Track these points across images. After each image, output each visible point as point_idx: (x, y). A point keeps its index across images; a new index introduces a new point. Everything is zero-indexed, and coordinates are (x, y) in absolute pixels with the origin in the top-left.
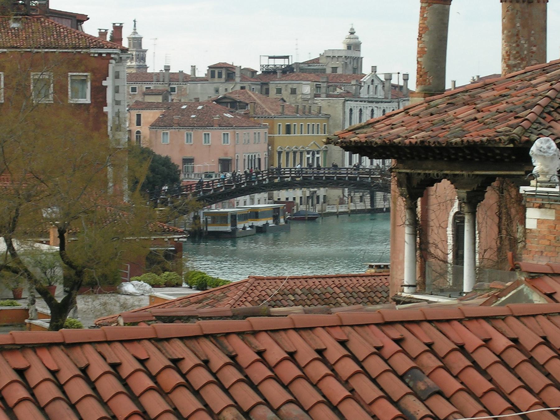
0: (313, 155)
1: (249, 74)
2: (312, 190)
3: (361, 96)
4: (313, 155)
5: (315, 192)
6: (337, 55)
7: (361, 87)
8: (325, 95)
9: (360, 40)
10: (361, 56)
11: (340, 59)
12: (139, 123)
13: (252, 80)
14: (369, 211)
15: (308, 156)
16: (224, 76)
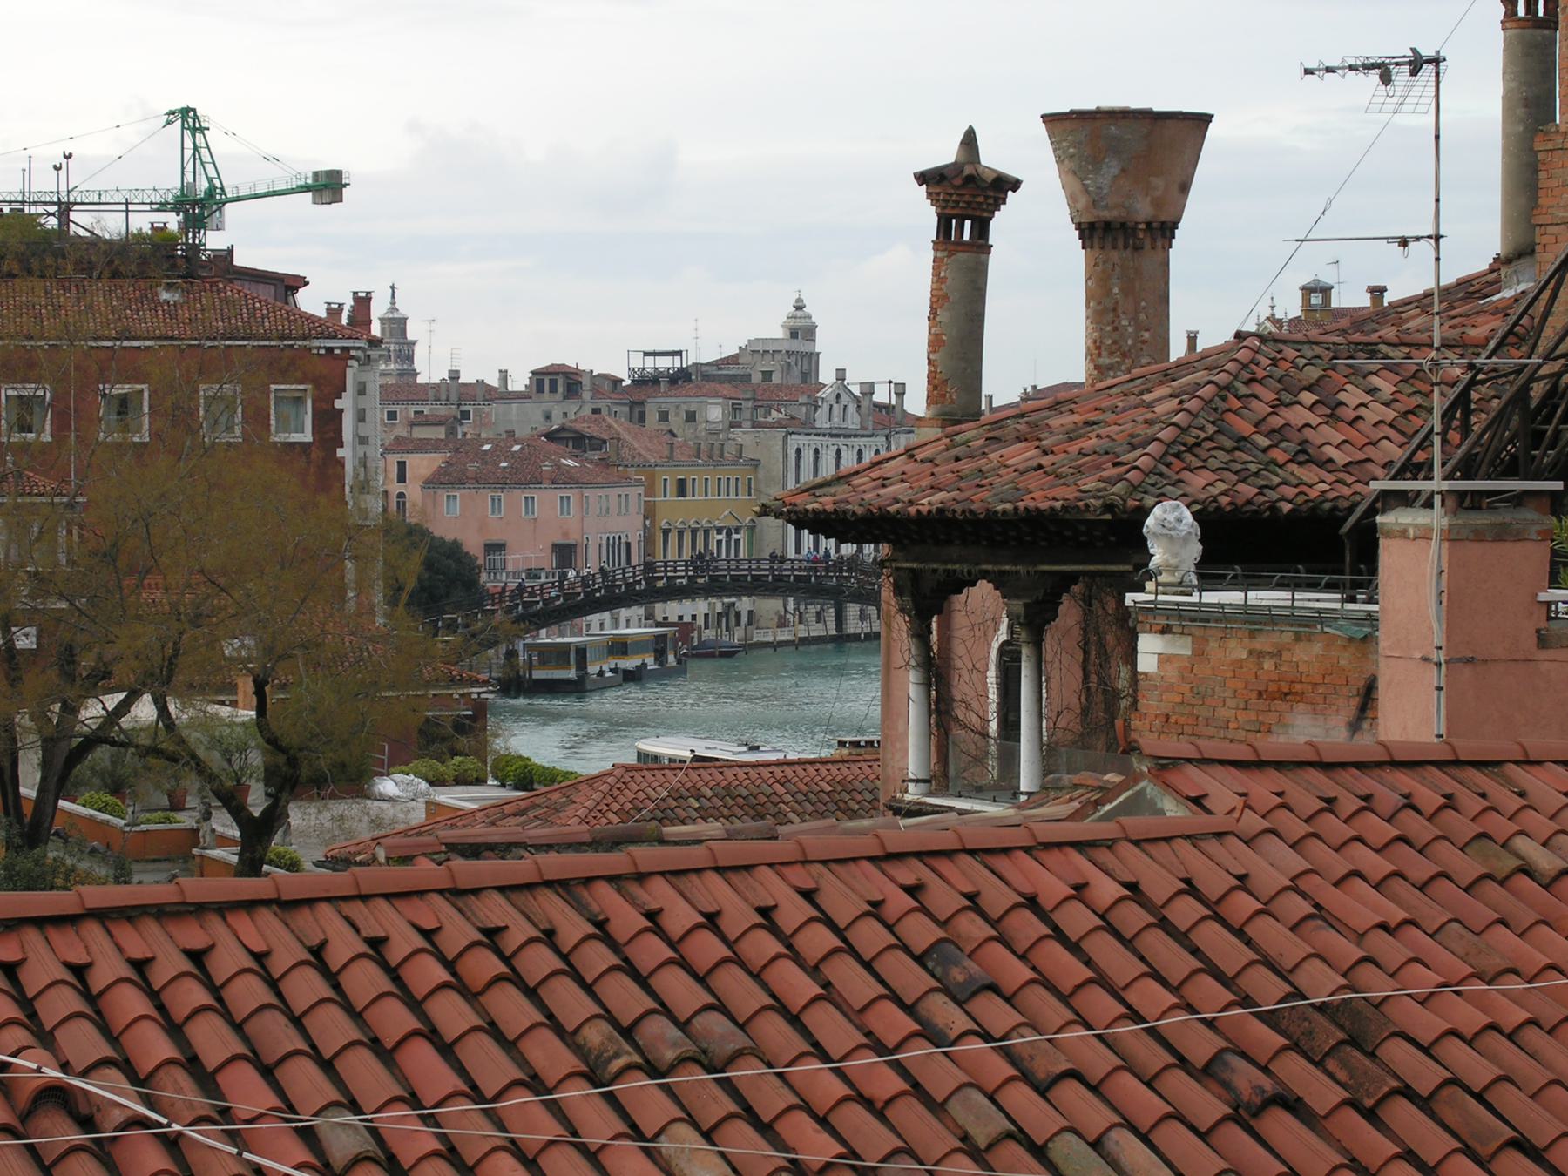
0: (729, 535)
1: (607, 386)
2: (726, 600)
3: (818, 424)
4: (729, 535)
5: (734, 604)
6: (771, 349)
7: (817, 408)
8: (749, 423)
9: (814, 320)
10: (817, 350)
11: (778, 357)
12: (402, 478)
13: (612, 395)
14: (833, 639)
15: (720, 537)
16: (560, 389)
